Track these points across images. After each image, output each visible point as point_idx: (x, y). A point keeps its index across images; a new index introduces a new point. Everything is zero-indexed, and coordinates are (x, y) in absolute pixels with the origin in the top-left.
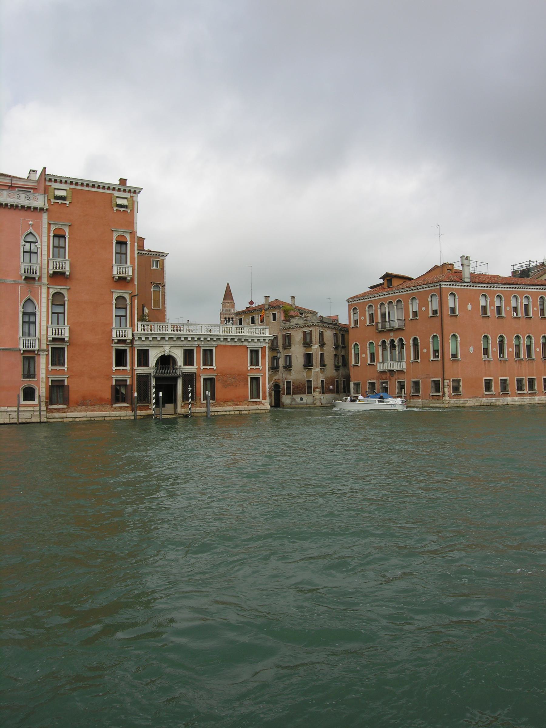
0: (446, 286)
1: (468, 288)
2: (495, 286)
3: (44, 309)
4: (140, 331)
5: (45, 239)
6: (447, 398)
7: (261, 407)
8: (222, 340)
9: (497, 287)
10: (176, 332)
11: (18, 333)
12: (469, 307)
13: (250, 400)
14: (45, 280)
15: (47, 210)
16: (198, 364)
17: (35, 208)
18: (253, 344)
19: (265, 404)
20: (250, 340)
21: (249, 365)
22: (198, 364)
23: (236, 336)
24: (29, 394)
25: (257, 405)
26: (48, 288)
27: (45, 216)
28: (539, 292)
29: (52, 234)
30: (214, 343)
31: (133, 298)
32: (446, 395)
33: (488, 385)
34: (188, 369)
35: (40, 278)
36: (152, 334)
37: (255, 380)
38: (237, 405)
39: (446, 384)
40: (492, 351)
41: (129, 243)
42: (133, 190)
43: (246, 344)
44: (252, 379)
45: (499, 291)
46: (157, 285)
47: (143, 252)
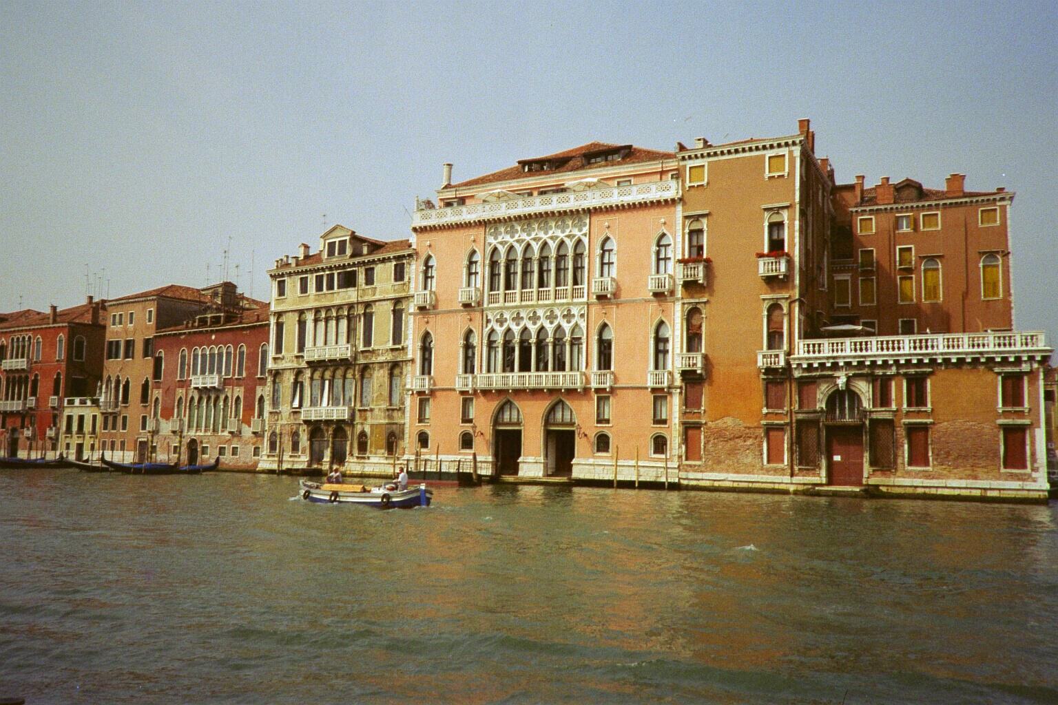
3: (678, 333)
4: (802, 355)
5: (679, 239)
7: (1030, 485)
10: (859, 353)
11: (647, 368)
14: (679, 292)
15: (681, 199)
16: (900, 404)
17: (666, 201)
19: (1039, 480)
21: (1000, 405)
22: (900, 404)
23: (967, 354)
24: (660, 444)
25: (1019, 480)
26: (684, 304)
27: (679, 208)
29: (687, 231)
31: (793, 305)
34: (882, 414)
35: (672, 293)
36: (816, 358)
38: (976, 478)
41: (786, 222)
42: (790, 142)
47: (964, 200)
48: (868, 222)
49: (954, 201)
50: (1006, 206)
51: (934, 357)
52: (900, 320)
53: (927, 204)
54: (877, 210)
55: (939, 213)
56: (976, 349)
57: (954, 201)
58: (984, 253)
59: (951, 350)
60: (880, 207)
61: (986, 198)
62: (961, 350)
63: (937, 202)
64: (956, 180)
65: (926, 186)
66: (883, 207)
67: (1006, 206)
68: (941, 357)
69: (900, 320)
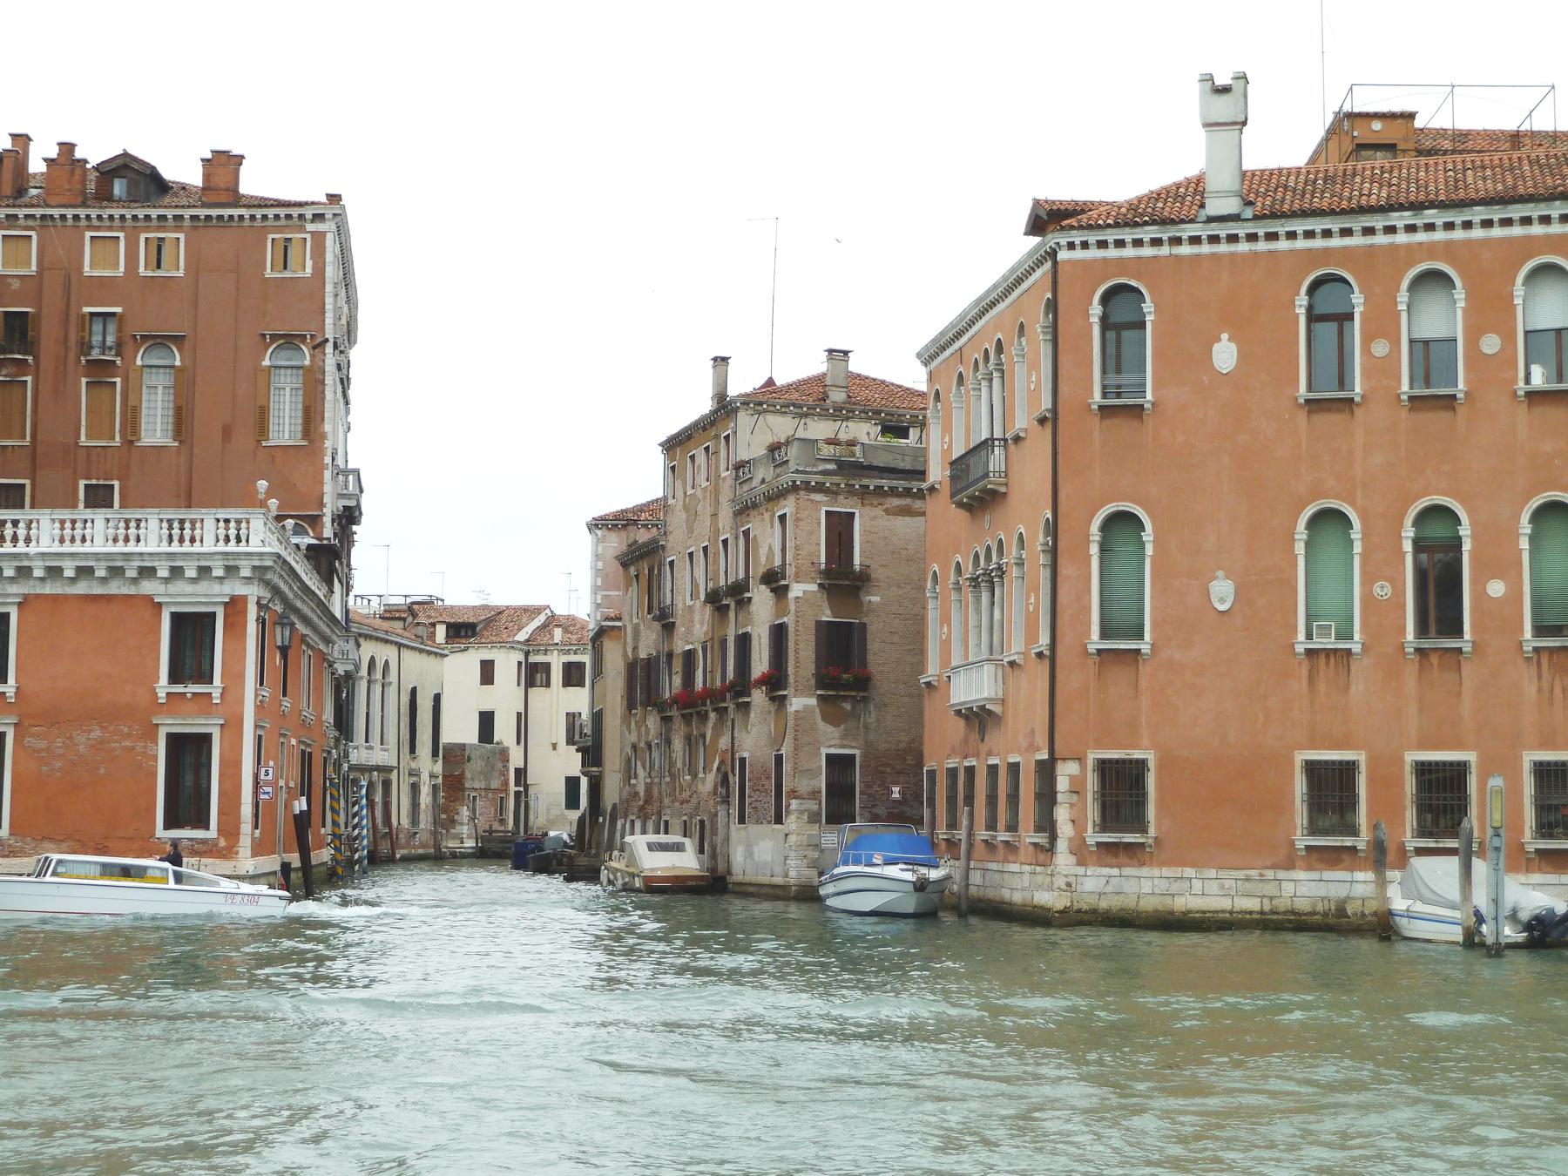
0: (1078, 254)
1: (1223, 248)
2: (1400, 219)
6: (1063, 859)
8: (38, 573)
9: (1411, 229)
12: (1225, 355)
13: (160, 832)
18: (180, 587)
20: (163, 573)
23: (97, 556)
28: (1529, 238)
30: (14, 589)
32: (1062, 845)
33: (1332, 789)
37: (188, 753)
39: (1062, 784)
40: (1368, 599)
43: (148, 587)
44: (175, 741)
45: (1431, 250)
46: (290, 341)
48: (22, 244)
49: (214, 212)
50: (324, 234)
51: (26, 563)
52: (82, 483)
53: (154, 213)
54: (43, 217)
55: (182, 236)
56: (120, 548)
57: (214, 212)
58: (274, 337)
59: (67, 548)
60: (49, 211)
61: (282, 212)
62: (87, 548)
63: (179, 212)
64: (223, 165)
65: (168, 174)
66: (56, 212)
67: (324, 234)
68: (40, 563)
69: (82, 483)
